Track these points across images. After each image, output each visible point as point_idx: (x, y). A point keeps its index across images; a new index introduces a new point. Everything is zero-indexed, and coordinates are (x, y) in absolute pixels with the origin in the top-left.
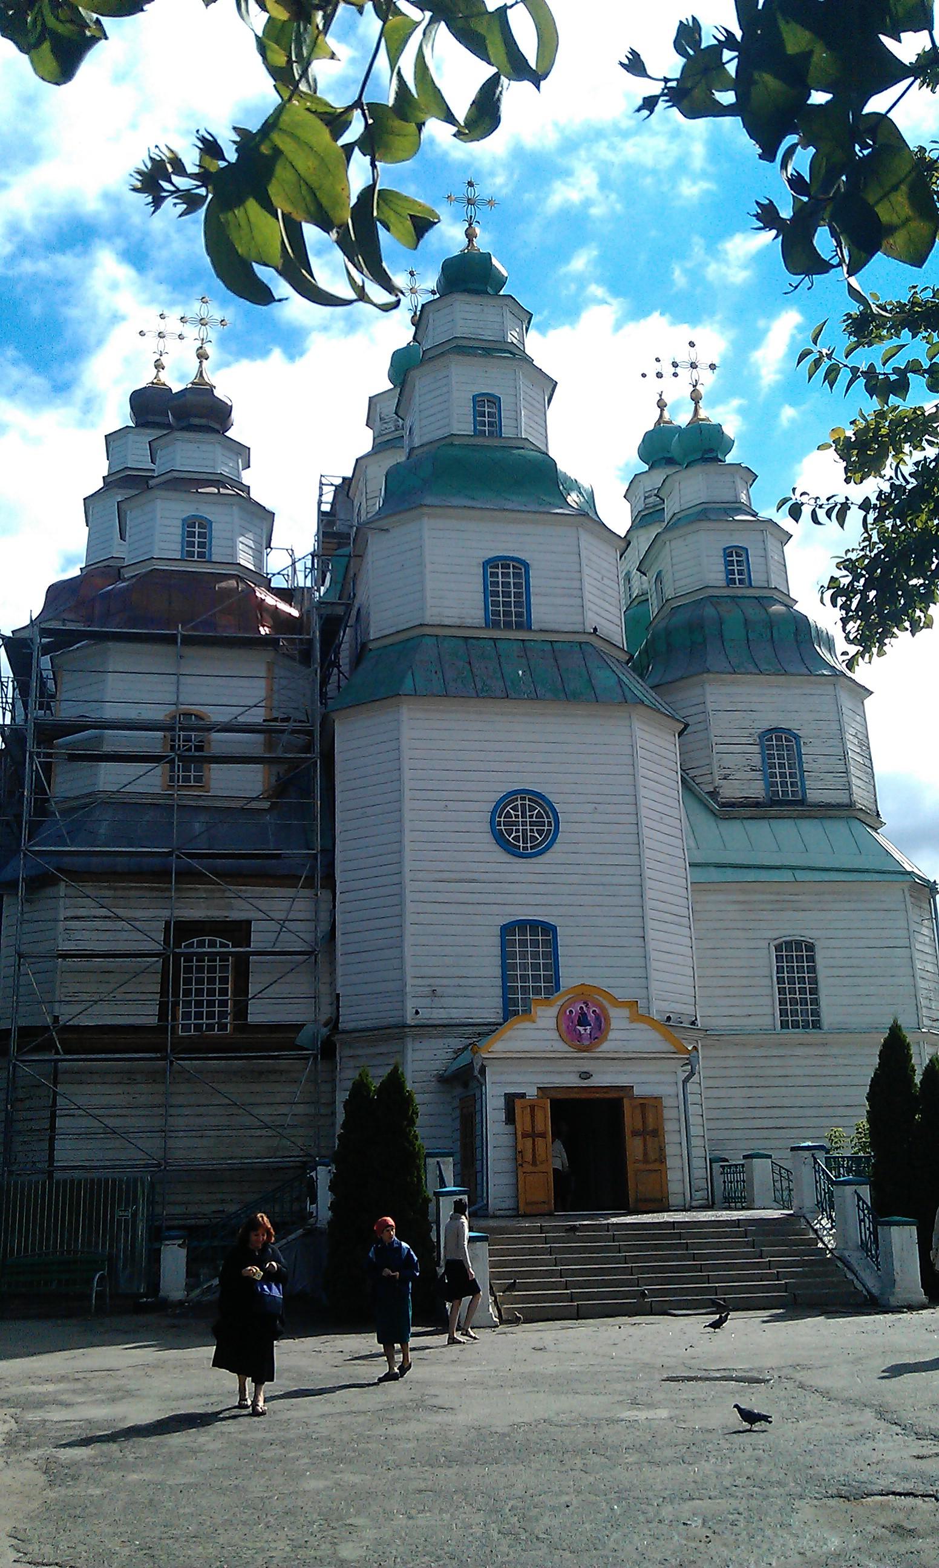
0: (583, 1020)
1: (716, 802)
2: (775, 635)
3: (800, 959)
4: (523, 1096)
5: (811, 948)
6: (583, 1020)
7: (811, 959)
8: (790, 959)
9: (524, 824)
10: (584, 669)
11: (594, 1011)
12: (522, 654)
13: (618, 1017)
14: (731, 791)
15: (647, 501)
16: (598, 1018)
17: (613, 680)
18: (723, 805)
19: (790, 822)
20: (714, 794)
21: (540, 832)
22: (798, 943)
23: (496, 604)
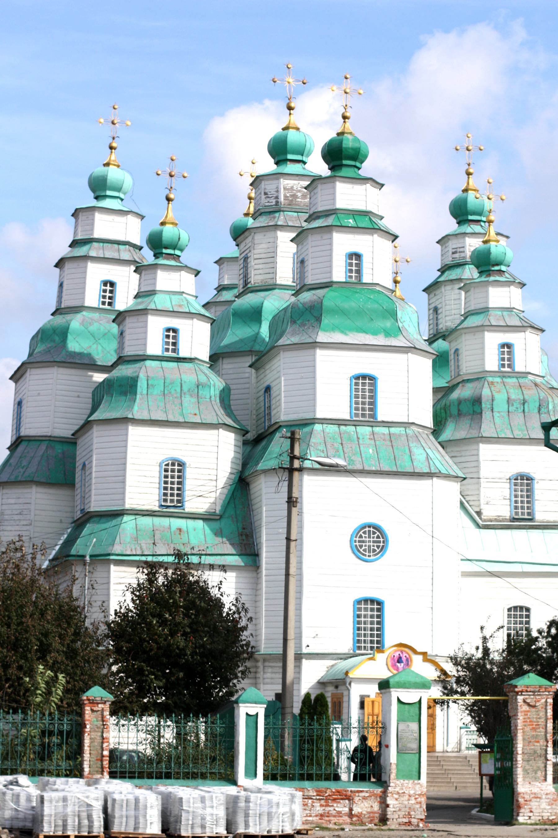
0: (399, 660)
1: (481, 519)
2: (526, 410)
3: (521, 617)
4: (369, 696)
5: (528, 610)
6: (399, 660)
7: (528, 616)
8: (515, 616)
9: (369, 541)
10: (407, 448)
11: (406, 656)
12: (372, 437)
13: (417, 660)
14: (489, 512)
15: (455, 256)
16: (407, 660)
17: (425, 455)
18: (485, 521)
19: (525, 530)
20: (479, 513)
21: (378, 547)
22: (521, 608)
23: (357, 409)
